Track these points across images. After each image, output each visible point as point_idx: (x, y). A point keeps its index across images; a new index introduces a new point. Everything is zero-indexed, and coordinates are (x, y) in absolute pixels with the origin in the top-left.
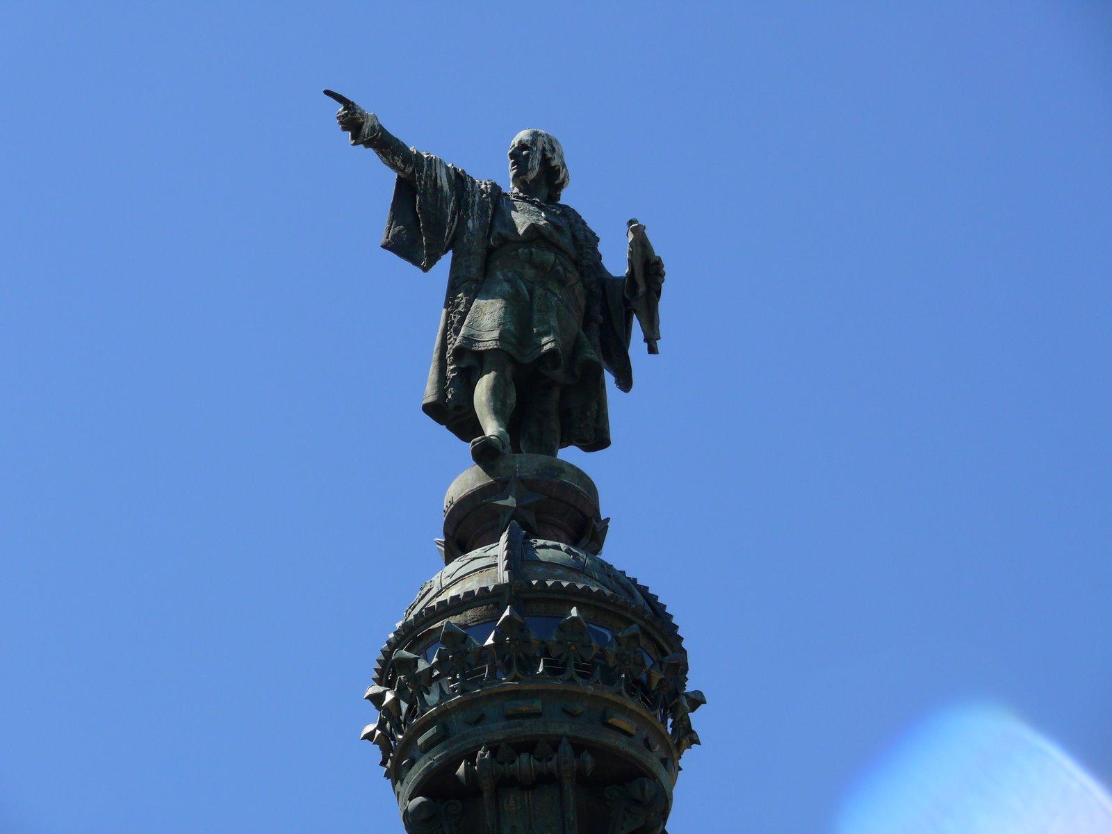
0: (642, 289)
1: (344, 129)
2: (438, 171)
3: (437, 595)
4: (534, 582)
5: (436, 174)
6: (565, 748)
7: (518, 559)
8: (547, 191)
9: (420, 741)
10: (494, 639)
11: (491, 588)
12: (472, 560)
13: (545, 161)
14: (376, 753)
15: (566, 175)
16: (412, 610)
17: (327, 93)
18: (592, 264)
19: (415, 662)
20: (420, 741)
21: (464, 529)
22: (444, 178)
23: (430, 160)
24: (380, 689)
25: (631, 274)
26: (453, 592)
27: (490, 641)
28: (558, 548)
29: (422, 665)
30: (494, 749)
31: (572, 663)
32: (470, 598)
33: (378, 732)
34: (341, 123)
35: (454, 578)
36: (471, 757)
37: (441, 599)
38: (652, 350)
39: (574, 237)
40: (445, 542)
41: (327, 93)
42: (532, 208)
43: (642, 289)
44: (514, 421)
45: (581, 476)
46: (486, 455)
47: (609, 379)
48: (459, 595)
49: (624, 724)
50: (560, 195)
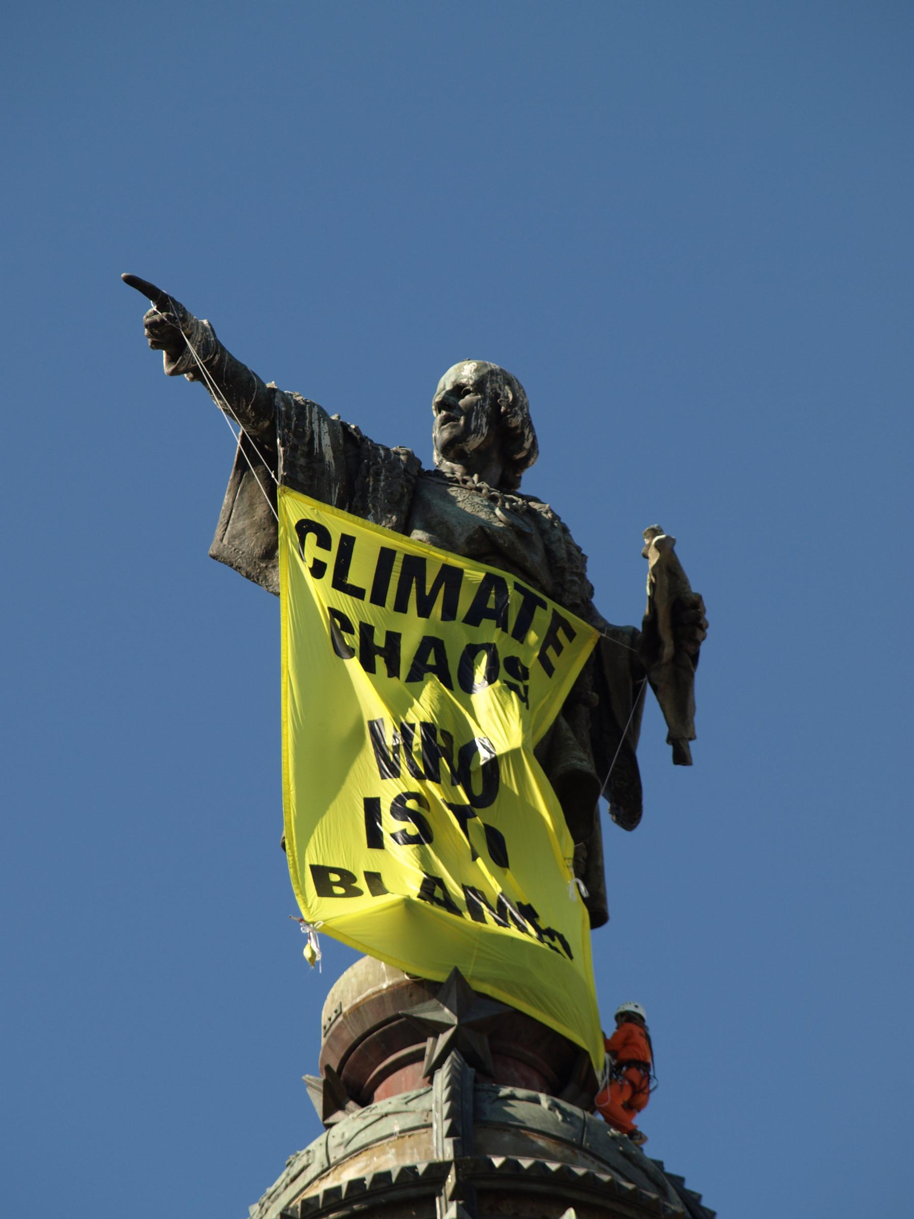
0: (668, 650)
1: (156, 345)
2: (315, 426)
4: (497, 1162)
5: (312, 432)
7: (471, 1119)
8: (500, 471)
11: (421, 1168)
12: (382, 1117)
13: (498, 420)
15: (534, 444)
16: (272, 1202)
17: (131, 281)
18: (579, 601)
22: (326, 440)
23: (301, 409)
32: (383, 1185)
34: (152, 334)
35: (351, 1148)
37: (329, 1183)
38: (681, 757)
39: (549, 553)
40: (326, 1083)
41: (131, 281)
42: (477, 500)
43: (668, 650)
47: (604, 805)
48: (364, 1179)
50: (520, 478)
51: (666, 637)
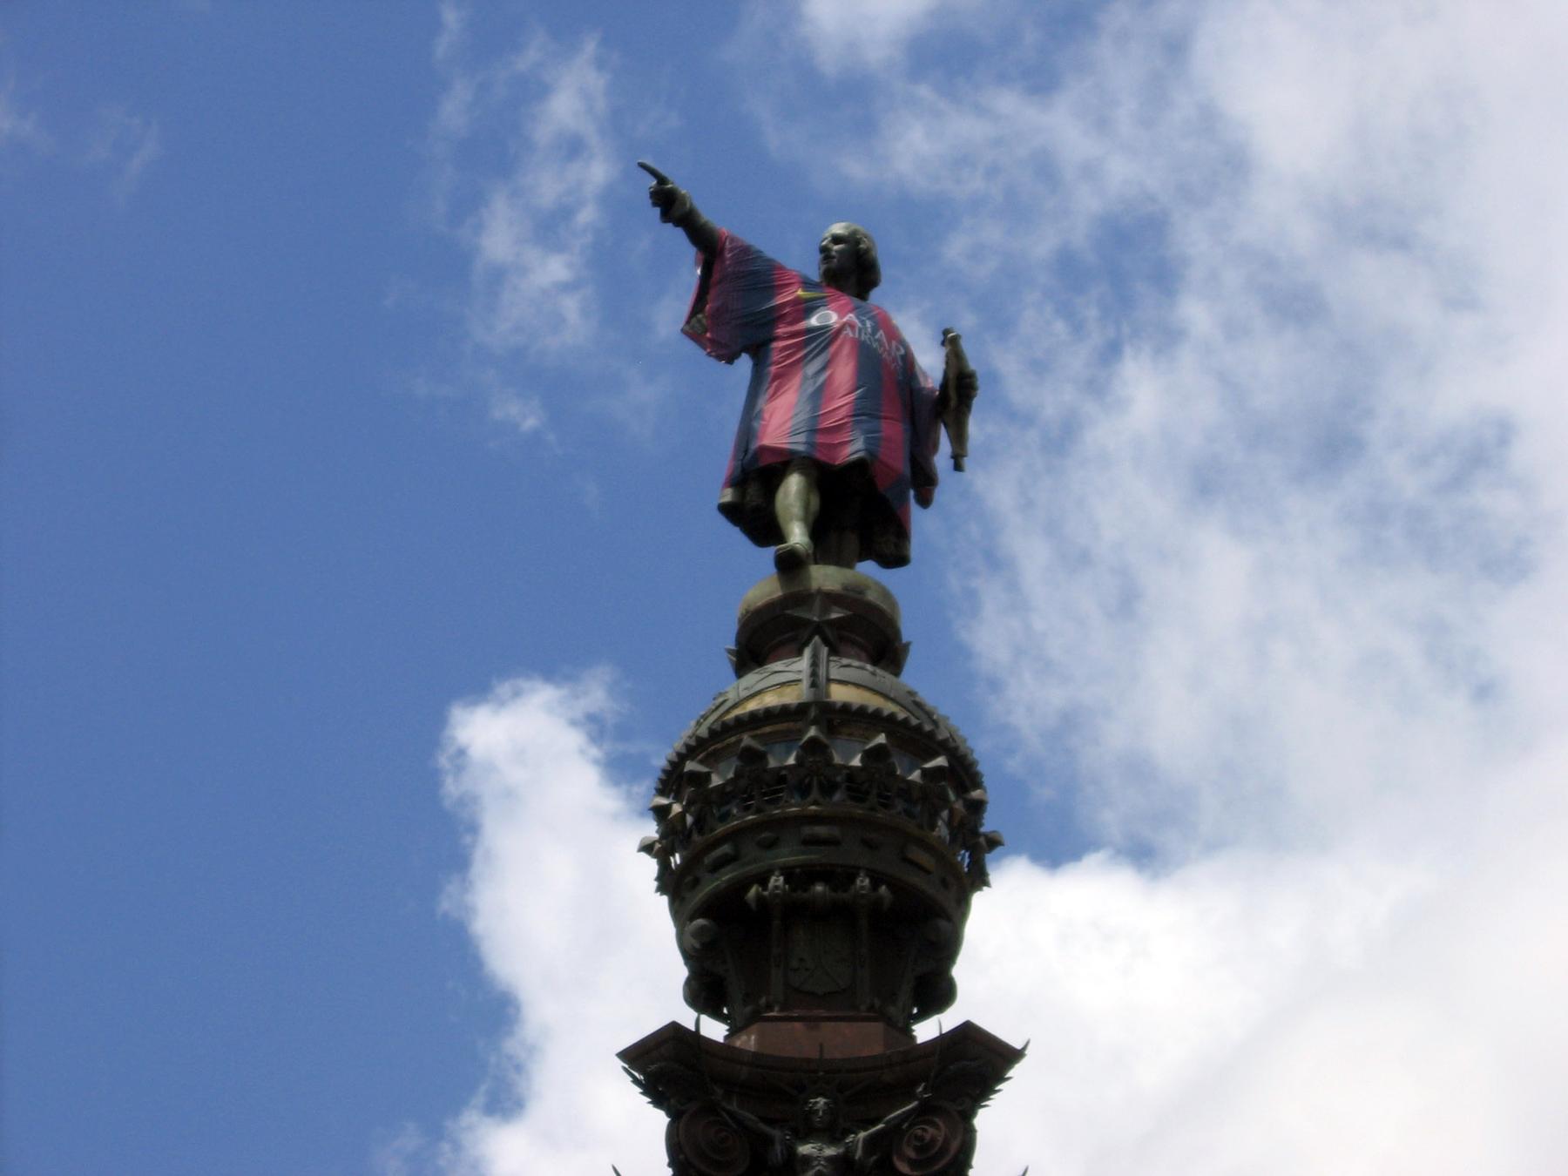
0: (953, 403)
3: (735, 706)
6: (863, 882)
9: (707, 860)
10: (797, 759)
14: (651, 866)
19: (707, 776)
20: (707, 860)
21: (759, 641)
24: (664, 801)
25: (944, 386)
26: (752, 706)
27: (791, 761)
28: (862, 668)
29: (716, 781)
30: (788, 872)
31: (875, 791)
33: (658, 846)
36: (763, 882)
38: (958, 467)
44: (817, 531)
45: (886, 594)
46: (789, 564)
49: (925, 859)
51: (952, 394)
